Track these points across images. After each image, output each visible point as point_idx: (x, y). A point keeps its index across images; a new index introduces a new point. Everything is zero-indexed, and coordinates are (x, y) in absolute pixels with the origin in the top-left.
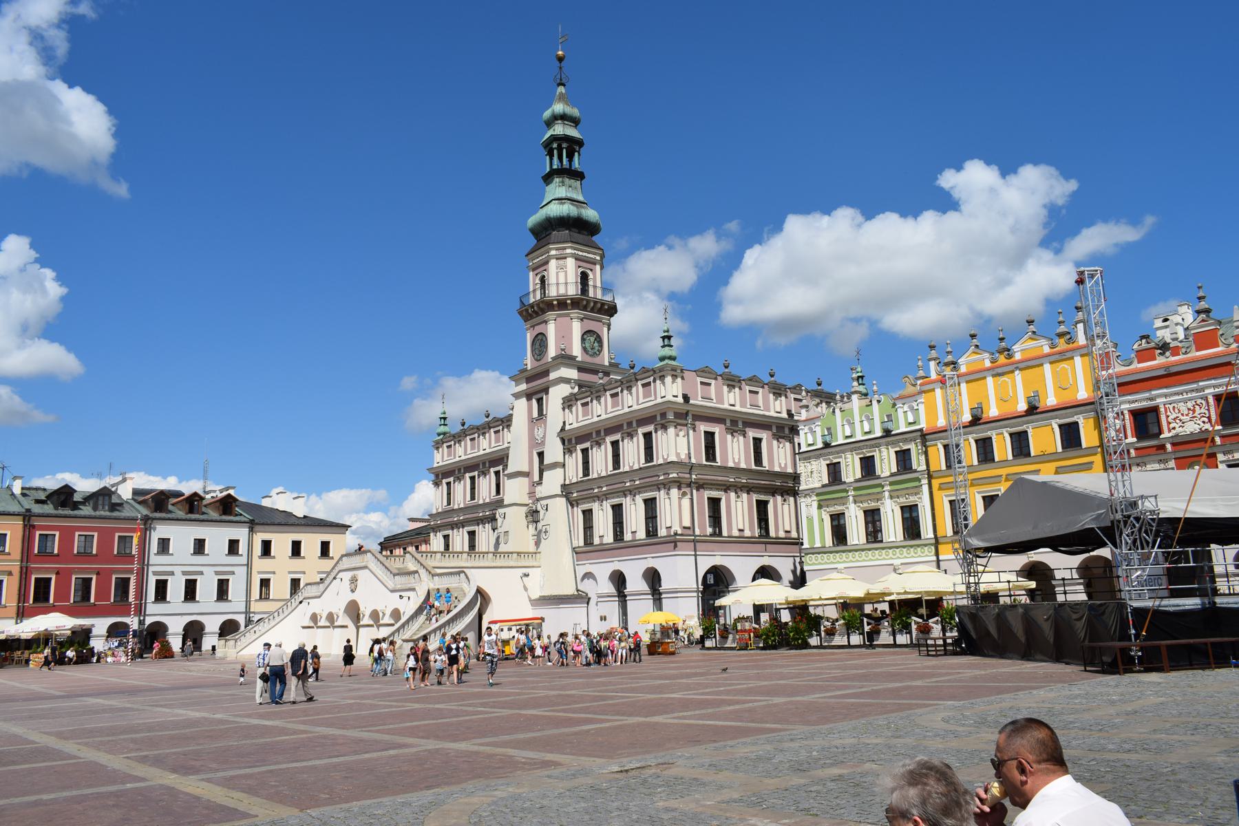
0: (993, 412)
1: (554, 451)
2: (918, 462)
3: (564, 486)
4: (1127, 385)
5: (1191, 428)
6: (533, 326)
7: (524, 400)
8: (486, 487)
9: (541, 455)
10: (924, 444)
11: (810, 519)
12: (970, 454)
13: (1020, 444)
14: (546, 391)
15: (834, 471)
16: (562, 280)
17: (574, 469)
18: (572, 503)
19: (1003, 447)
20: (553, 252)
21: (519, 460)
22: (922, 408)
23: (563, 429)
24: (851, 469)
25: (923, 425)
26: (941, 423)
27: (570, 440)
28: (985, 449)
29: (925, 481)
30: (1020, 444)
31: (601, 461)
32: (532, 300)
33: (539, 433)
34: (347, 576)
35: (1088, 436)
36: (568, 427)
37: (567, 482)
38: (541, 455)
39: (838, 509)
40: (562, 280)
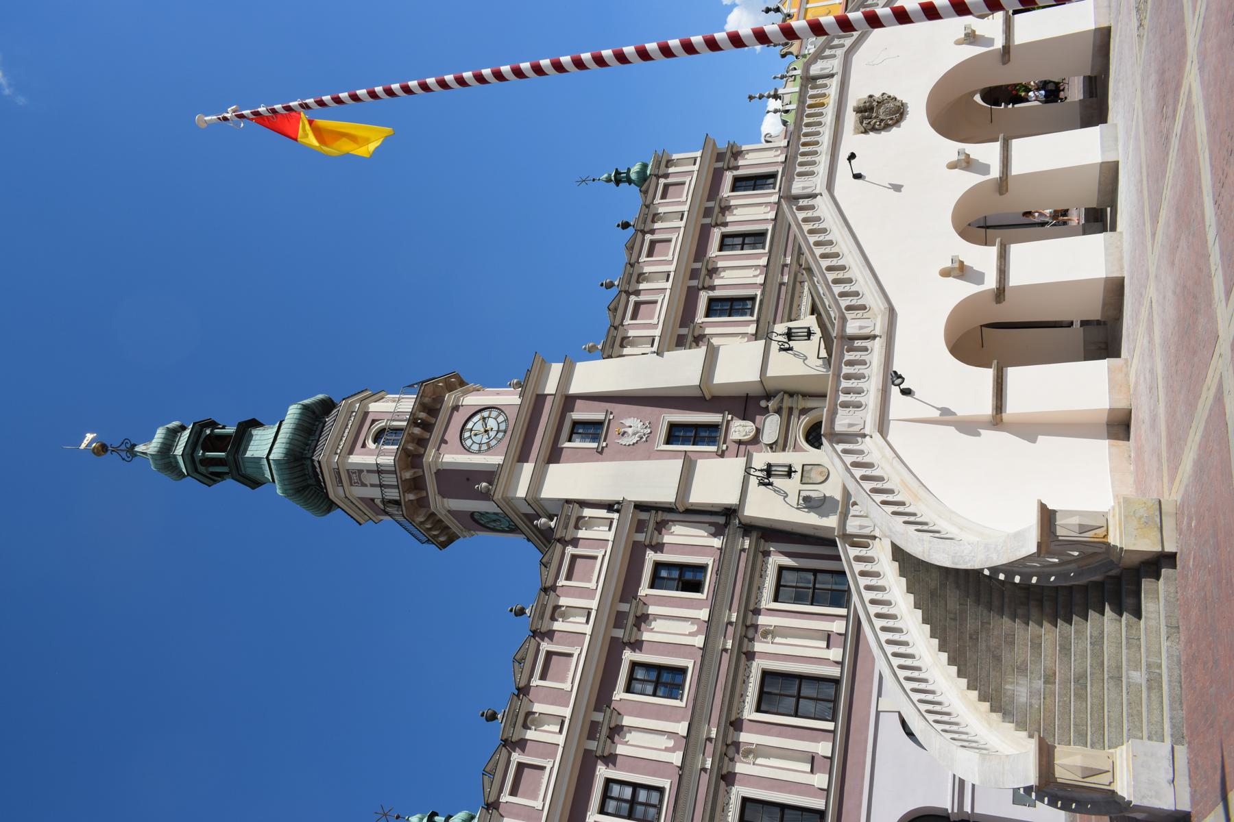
6: (443, 441)
7: (553, 467)
8: (675, 627)
9: (676, 433)
14: (569, 401)
21: (654, 479)
31: (739, 273)
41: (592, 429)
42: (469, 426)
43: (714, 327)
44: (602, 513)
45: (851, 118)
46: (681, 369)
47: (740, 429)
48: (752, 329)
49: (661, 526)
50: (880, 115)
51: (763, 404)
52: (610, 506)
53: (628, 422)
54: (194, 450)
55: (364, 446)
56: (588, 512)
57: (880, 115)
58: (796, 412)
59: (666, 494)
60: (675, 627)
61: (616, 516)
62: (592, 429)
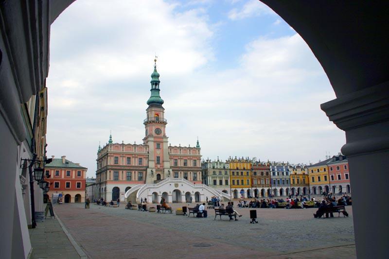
0: (239, 168)
1: (167, 157)
2: (228, 173)
4: (255, 169)
5: (259, 175)
7: (153, 143)
9: (158, 158)
11: (210, 180)
12: (235, 174)
13: (242, 173)
15: (214, 172)
18: (173, 170)
19: (240, 174)
21: (152, 157)
24: (217, 173)
28: (238, 173)
30: (242, 173)
32: (153, 119)
35: (249, 174)
38: (158, 158)
39: (215, 179)
43: (172, 161)
48: (172, 166)
50: (176, 185)
57: (176, 185)
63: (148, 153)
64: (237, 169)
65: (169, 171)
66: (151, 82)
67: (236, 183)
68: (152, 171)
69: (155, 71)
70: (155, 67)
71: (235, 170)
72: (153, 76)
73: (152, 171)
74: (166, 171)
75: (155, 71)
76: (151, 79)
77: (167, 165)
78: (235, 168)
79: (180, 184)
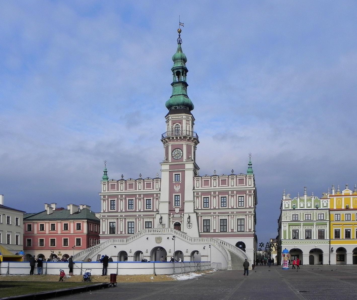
3: (194, 210)
10: (329, 213)
16: (188, 129)
17: (199, 203)
20: (184, 117)
22: (329, 203)
23: (194, 189)
25: (329, 208)
26: (335, 208)
27: (198, 193)
29: (328, 224)
31: (215, 202)
33: (177, 188)
34: (155, 236)
36: (196, 188)
37: (196, 209)
40: (188, 129)
41: (177, 180)
42: (178, 150)
44: (159, 187)
45: (158, 236)
46: (189, 195)
47: (177, 210)
49: (157, 199)
50: (159, 240)
51: (183, 213)
52: (160, 189)
53: (179, 186)
54: (176, 69)
55: (174, 123)
56: (159, 183)
57: (159, 240)
58: (181, 220)
59: (162, 199)
60: (140, 205)
61: (159, 190)
62: (177, 180)
63: (160, 190)
64: (347, 209)
65: (189, 217)
66: (173, 70)
67: (343, 235)
68: (161, 218)
69: (180, 49)
70: (180, 43)
71: (342, 210)
72: (175, 60)
73: (161, 218)
74: (186, 216)
75: (180, 49)
76: (172, 65)
77: (189, 208)
78: (343, 208)
79: (164, 238)
